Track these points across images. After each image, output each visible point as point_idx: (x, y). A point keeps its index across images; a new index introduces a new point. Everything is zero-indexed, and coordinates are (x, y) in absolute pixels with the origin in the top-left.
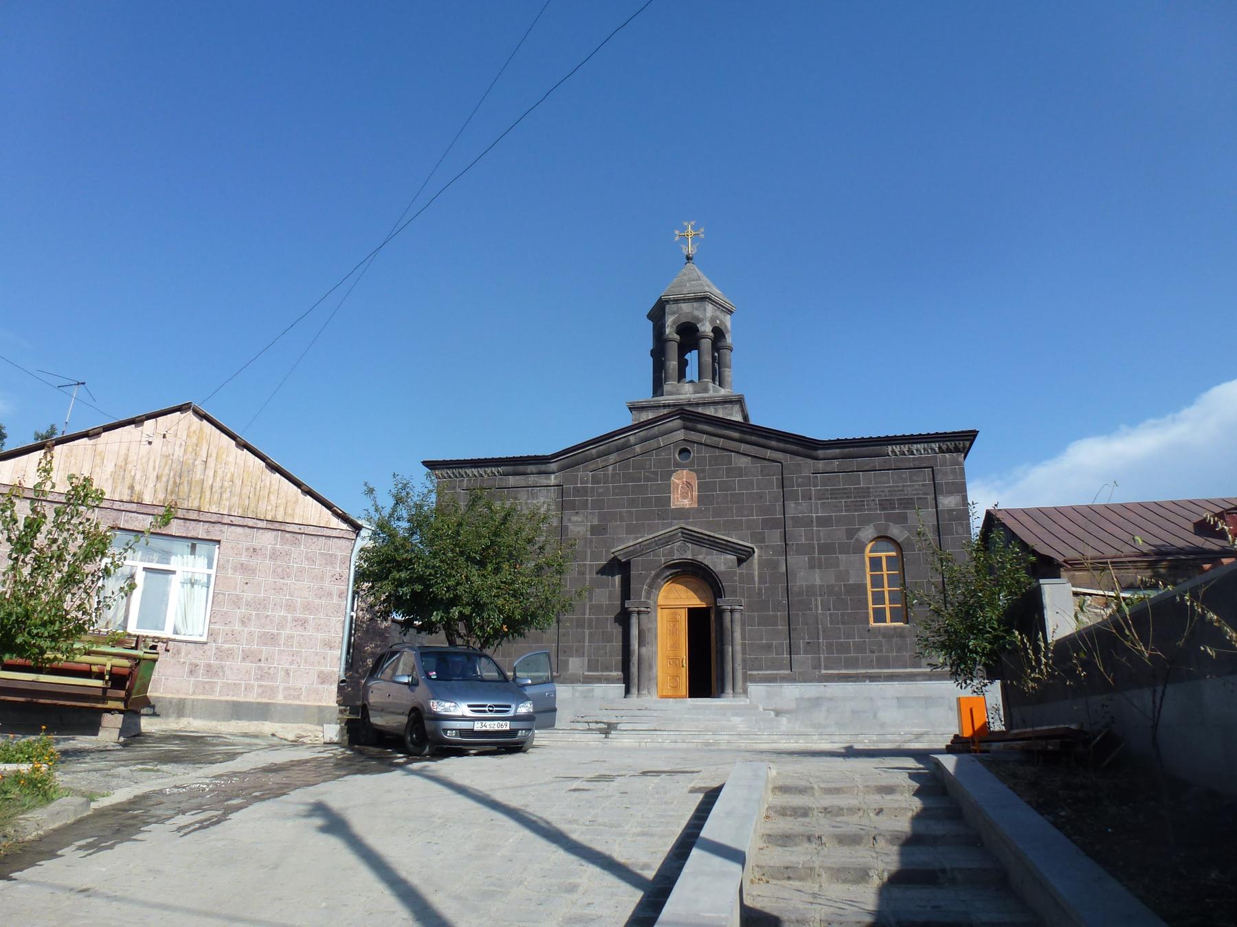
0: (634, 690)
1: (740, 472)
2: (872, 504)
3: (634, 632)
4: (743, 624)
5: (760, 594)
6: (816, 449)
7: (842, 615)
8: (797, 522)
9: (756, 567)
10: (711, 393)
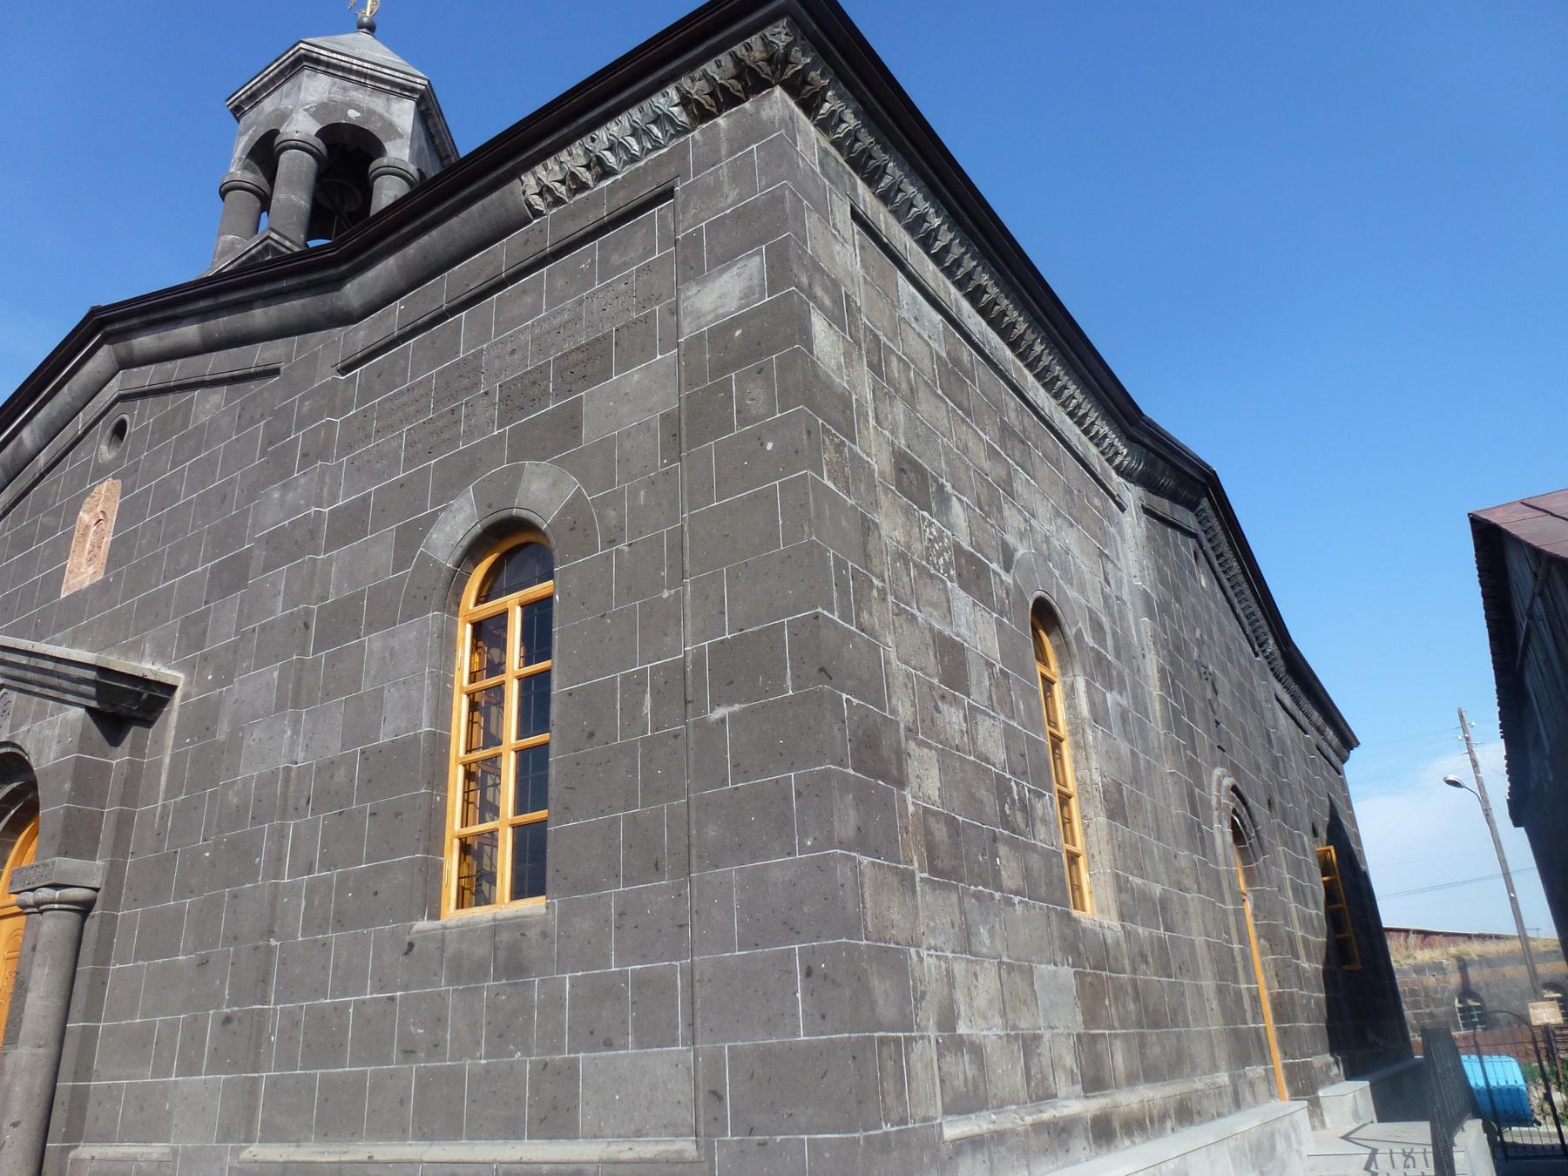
6: (338, 283)
7: (343, 879)
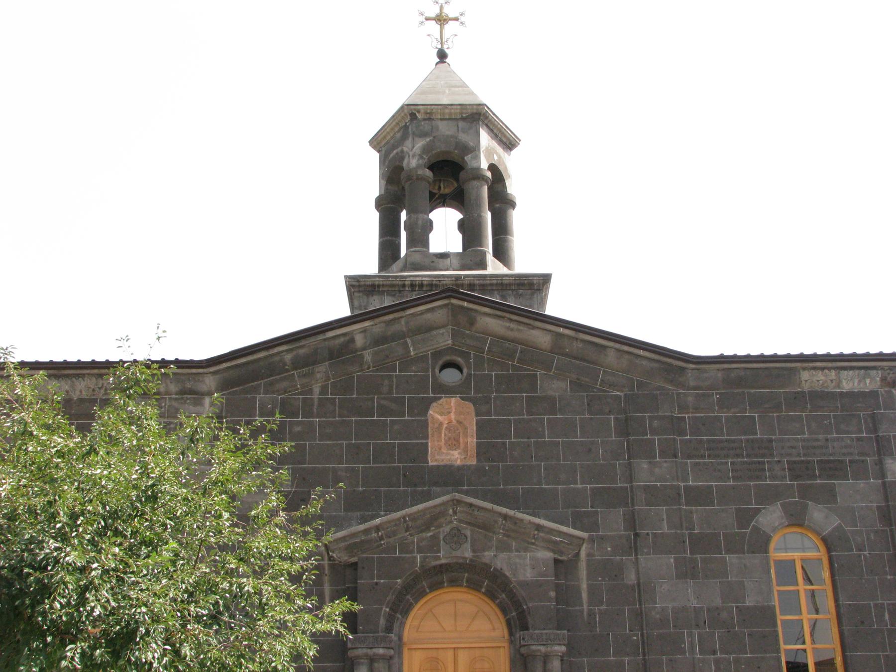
1: (552, 405)
2: (777, 468)
7: (737, 661)
8: (654, 495)
10: (490, 271)
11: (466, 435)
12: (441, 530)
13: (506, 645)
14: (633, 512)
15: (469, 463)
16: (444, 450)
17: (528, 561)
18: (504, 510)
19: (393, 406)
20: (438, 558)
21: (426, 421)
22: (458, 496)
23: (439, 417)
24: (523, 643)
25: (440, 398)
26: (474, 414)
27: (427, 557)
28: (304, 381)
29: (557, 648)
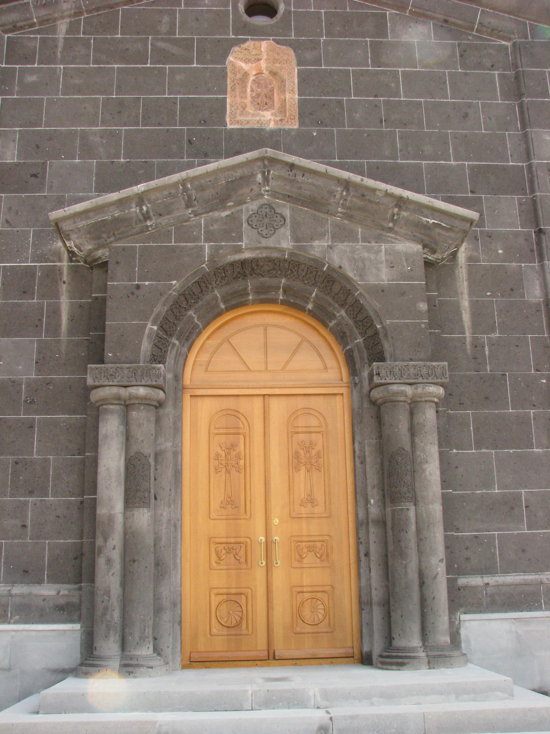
0: (109, 647)
3: (111, 461)
4: (445, 441)
5: (477, 357)
9: (463, 285)
11: (282, 90)
12: (244, 207)
13: (344, 390)
14: (534, 202)
15: (287, 127)
16: (250, 109)
17: (382, 256)
18: (345, 175)
19: (175, 50)
20: (239, 250)
21: (224, 70)
22: (270, 152)
23: (243, 65)
24: (376, 380)
25: (245, 41)
26: (294, 62)
27: (221, 247)
28: (43, 12)
29: (432, 389)
